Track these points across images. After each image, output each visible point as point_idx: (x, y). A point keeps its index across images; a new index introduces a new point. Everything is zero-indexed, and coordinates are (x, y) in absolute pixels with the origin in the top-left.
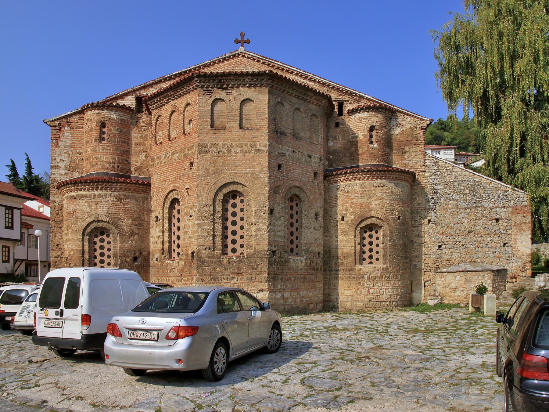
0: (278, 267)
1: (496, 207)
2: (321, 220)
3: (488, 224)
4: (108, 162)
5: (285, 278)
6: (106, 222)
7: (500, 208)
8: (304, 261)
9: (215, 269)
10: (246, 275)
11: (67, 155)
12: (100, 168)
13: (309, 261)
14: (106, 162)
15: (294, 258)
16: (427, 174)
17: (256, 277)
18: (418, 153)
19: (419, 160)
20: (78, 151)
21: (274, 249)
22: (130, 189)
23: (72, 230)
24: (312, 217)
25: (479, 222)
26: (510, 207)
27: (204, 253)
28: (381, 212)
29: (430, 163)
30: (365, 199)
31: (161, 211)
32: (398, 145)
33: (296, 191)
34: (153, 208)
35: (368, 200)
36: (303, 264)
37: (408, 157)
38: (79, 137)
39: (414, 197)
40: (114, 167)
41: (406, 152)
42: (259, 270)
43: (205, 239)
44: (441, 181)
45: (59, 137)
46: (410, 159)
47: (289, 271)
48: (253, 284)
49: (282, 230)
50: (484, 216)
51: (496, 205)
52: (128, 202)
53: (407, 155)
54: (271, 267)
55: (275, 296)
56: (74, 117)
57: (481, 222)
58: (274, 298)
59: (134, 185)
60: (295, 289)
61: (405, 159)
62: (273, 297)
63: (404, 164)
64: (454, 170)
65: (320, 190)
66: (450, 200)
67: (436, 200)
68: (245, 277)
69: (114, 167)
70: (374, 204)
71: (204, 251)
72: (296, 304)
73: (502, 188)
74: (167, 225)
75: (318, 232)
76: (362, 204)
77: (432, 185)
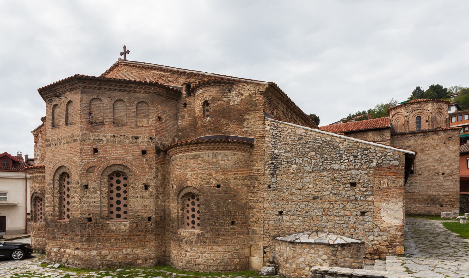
1: (350, 169)
3: (339, 189)
7: (357, 169)
16: (267, 140)
18: (257, 119)
25: (327, 186)
26: (371, 168)
28: (196, 181)
29: (270, 128)
32: (238, 114)
35: (185, 171)
37: (247, 125)
39: (253, 163)
41: (245, 120)
44: (282, 144)
46: (249, 126)
50: (333, 180)
51: (351, 167)
53: (246, 123)
57: (331, 186)
61: (244, 127)
63: (243, 132)
66: (292, 163)
67: (276, 165)
73: (360, 146)
76: (181, 175)
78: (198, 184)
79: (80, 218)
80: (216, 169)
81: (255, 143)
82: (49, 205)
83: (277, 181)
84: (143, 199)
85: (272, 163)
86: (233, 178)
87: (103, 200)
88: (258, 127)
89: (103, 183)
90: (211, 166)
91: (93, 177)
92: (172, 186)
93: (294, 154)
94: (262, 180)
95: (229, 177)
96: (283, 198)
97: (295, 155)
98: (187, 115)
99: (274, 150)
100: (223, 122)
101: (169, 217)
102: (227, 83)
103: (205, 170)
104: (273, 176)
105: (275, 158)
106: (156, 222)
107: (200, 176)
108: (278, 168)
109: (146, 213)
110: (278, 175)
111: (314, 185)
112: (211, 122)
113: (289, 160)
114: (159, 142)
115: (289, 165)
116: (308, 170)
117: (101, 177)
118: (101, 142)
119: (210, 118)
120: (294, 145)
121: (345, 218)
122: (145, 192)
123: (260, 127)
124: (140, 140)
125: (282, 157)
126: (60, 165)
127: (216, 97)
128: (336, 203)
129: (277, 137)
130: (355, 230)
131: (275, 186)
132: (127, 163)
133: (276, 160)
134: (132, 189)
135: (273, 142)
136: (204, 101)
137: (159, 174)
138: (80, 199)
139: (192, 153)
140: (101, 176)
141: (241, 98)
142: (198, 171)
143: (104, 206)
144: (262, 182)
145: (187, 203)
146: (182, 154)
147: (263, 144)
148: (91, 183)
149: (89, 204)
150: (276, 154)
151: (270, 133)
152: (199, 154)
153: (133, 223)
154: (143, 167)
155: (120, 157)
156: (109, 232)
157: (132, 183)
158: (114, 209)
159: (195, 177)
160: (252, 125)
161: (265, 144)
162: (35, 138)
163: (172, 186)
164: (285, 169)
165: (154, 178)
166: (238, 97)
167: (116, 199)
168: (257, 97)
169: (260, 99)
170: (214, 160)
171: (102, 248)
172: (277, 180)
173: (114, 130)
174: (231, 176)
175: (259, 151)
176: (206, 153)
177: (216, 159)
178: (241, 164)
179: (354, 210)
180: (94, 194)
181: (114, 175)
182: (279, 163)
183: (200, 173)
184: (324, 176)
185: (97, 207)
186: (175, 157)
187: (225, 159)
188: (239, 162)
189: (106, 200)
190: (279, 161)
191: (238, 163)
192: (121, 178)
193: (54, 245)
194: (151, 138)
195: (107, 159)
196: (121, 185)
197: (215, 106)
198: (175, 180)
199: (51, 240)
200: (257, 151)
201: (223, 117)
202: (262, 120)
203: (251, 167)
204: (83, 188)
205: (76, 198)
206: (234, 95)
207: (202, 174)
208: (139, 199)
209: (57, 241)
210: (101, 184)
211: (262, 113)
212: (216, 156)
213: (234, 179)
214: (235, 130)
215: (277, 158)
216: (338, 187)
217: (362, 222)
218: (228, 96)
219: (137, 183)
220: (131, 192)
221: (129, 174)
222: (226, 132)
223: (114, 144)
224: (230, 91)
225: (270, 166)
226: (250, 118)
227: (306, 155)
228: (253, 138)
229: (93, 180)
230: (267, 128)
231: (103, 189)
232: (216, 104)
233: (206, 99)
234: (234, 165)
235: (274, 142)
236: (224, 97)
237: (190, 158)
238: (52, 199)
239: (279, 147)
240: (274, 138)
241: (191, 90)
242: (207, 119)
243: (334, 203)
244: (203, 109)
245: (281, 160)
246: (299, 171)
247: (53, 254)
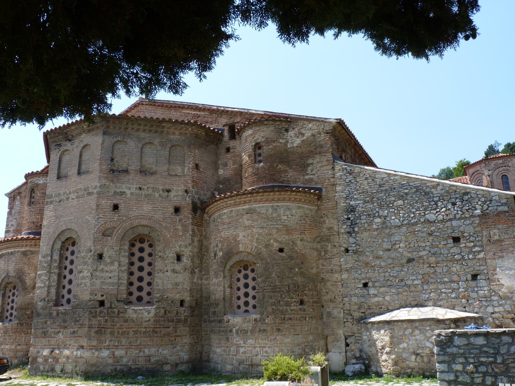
0: (106, 319)
5: (118, 332)
9: (46, 322)
13: (162, 311)
15: (136, 308)
16: (339, 188)
17: (77, 331)
18: (324, 164)
19: (326, 172)
21: (101, 299)
24: (170, 258)
29: (341, 173)
30: (231, 231)
33: (146, 231)
35: (235, 231)
36: (152, 315)
37: (312, 171)
39: (322, 219)
41: (308, 165)
42: (81, 322)
43: (42, 290)
44: (360, 193)
46: (314, 172)
47: (126, 324)
53: (310, 168)
54: (94, 320)
58: (97, 357)
60: (134, 346)
61: (308, 174)
63: (306, 180)
64: (377, 176)
65: (184, 226)
71: (40, 303)
75: (182, 275)
78: (254, 248)
79: (90, 301)
80: (277, 226)
81: (324, 193)
83: (357, 242)
84: (174, 273)
85: (349, 219)
86: (299, 239)
87: (121, 275)
88: (326, 173)
89: (123, 251)
90: (270, 223)
91: (111, 243)
92: (213, 255)
93: (375, 204)
94: (336, 241)
95: (294, 237)
96: (367, 264)
97: (377, 206)
99: (349, 201)
100: (280, 168)
101: (207, 301)
102: (284, 121)
103: (263, 228)
104: (351, 235)
105: (352, 211)
106: (191, 307)
107: (256, 236)
108: (356, 224)
109: (178, 293)
110: (357, 233)
111: (406, 244)
112: (265, 169)
113: (370, 213)
114: (196, 196)
115: (371, 219)
116: (397, 224)
117: (120, 243)
118: (123, 196)
119: (263, 163)
120: (375, 194)
121: (452, 285)
122: (177, 263)
123: (328, 173)
125: (360, 210)
127: (270, 138)
128: (438, 265)
129: (351, 185)
130: (468, 301)
131: (355, 248)
132: (155, 223)
133: (352, 213)
134: (160, 259)
135: (348, 191)
136: (255, 143)
137: (196, 239)
138: (92, 274)
140: (121, 241)
141: (301, 139)
142: (254, 230)
143: (121, 283)
144: (337, 245)
145: (237, 277)
146: (230, 209)
147: (334, 194)
148: (107, 251)
149: (102, 280)
150: (352, 206)
151: (342, 180)
152: (254, 208)
153: (160, 308)
154: (176, 229)
157: (160, 252)
158: (134, 289)
160: (318, 170)
161: (336, 194)
162: (11, 202)
163: (215, 255)
164: (366, 225)
165: (190, 244)
166: (298, 137)
167: (137, 274)
170: (274, 215)
172: (357, 240)
173: (140, 178)
174: (296, 236)
175: (330, 204)
176: (264, 206)
177: (277, 215)
178: (307, 220)
179: (462, 273)
180: (111, 266)
181: (136, 241)
182: (357, 217)
183: (256, 233)
184: (417, 231)
186: (220, 214)
187: (288, 213)
188: (306, 218)
189: (125, 275)
190: (357, 215)
191: (305, 219)
192: (145, 245)
194: (186, 191)
196: (145, 255)
197: (270, 149)
198: (220, 245)
200: (327, 205)
201: (281, 162)
202: (331, 165)
203: (320, 225)
204: (96, 258)
205: (86, 272)
206: (293, 135)
208: (169, 274)
210: (120, 253)
211: (330, 156)
212: (276, 209)
213: (301, 240)
214: (296, 178)
215: (354, 211)
216: (438, 243)
217: (476, 289)
218: (285, 137)
219: (167, 252)
220: (159, 264)
221: (157, 238)
222: (285, 181)
223: (139, 197)
224: (287, 130)
225: (346, 221)
226: (315, 162)
227: (391, 205)
228: (320, 187)
229: (110, 246)
230: (337, 174)
231: (122, 259)
232: (271, 147)
233: (258, 141)
234: (300, 222)
235: (349, 190)
236: (281, 138)
237: (242, 213)
238: (48, 276)
239: (355, 197)
240: (348, 185)
241: (234, 133)
242: (260, 165)
243: (435, 265)
244: (255, 153)
245: (359, 213)
246: (384, 226)
247: (40, 360)
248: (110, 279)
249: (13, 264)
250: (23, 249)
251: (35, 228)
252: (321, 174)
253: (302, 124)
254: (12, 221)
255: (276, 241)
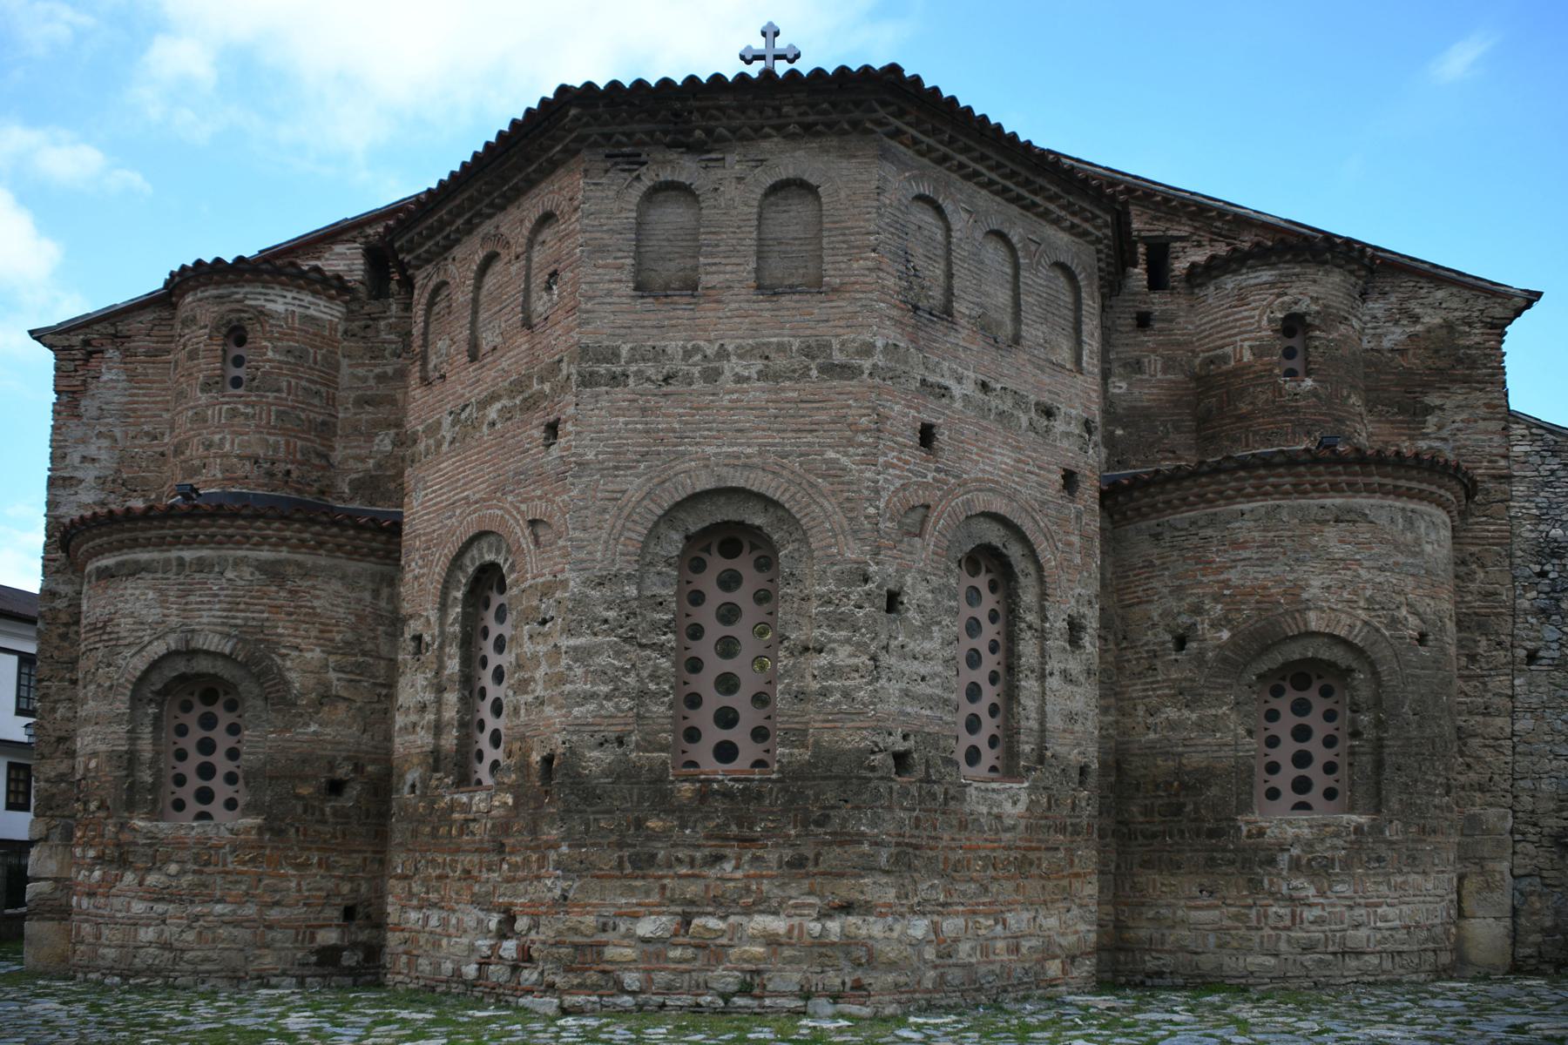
2: (1089, 648)
4: (248, 458)
6: (222, 655)
8: (1024, 798)
9: (639, 824)
10: (776, 845)
11: (105, 443)
12: (219, 476)
14: (238, 456)
17: (818, 855)
20: (146, 428)
21: (901, 746)
22: (321, 544)
23: (99, 685)
27: (596, 760)
31: (433, 616)
32: (1396, 385)
34: (406, 608)
35: (1292, 571)
37: (1440, 428)
38: (154, 382)
40: (271, 475)
41: (1429, 410)
45: (84, 382)
46: (1445, 433)
48: (806, 884)
49: (935, 675)
52: (314, 587)
53: (1432, 420)
55: (904, 933)
56: (141, 318)
59: (335, 530)
62: (895, 935)
68: (772, 857)
69: (271, 475)
70: (1315, 587)
72: (992, 962)
74: (453, 665)
76: (1265, 588)
77: (1541, 527)
79: (873, 752)
82: (605, 689)
88: (1484, 441)
90: (1401, 559)
98: (1154, 363)
107: (1368, 593)
124: (1059, 426)
126: (705, 483)
134: (1029, 634)
139: (1328, 502)
155: (1002, 481)
156: (966, 828)
159: (1346, 595)
168: (1475, 334)
169: (1487, 344)
170: (1409, 536)
171: (944, 905)
183: (1367, 581)
185: (932, 704)
187: (1433, 537)
193: (639, 905)
195: (965, 483)
199: (611, 877)
207: (1378, 586)
209: (666, 881)
214: (1387, 443)
230: (1515, 449)
248: (923, 684)
249: (217, 607)
250: (265, 554)
251: (266, 481)
252: (1468, 443)
253: (1412, 284)
254: (84, 441)
255: (1416, 613)
